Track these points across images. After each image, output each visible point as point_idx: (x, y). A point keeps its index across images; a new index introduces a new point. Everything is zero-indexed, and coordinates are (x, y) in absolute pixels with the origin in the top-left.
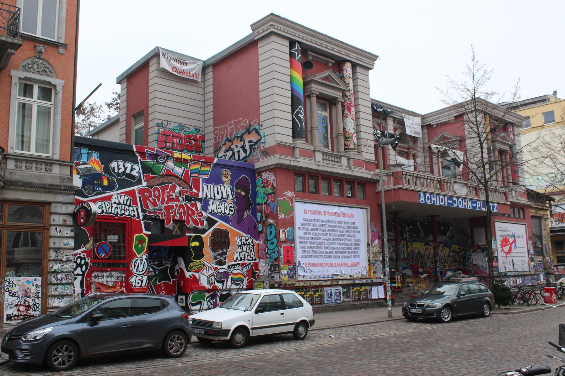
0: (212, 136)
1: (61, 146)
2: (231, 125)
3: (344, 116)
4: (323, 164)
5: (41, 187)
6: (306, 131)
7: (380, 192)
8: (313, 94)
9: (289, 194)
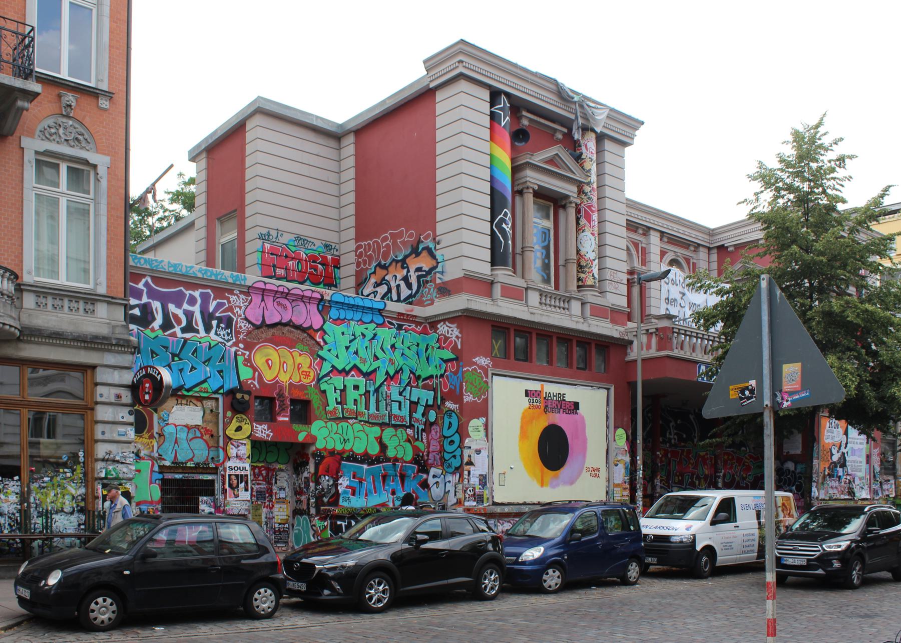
0: (352, 258)
1: (108, 271)
2: (385, 239)
3: (579, 229)
4: (540, 312)
5: (78, 341)
6: (514, 254)
7: (635, 361)
8: (528, 188)
9: (483, 361)
